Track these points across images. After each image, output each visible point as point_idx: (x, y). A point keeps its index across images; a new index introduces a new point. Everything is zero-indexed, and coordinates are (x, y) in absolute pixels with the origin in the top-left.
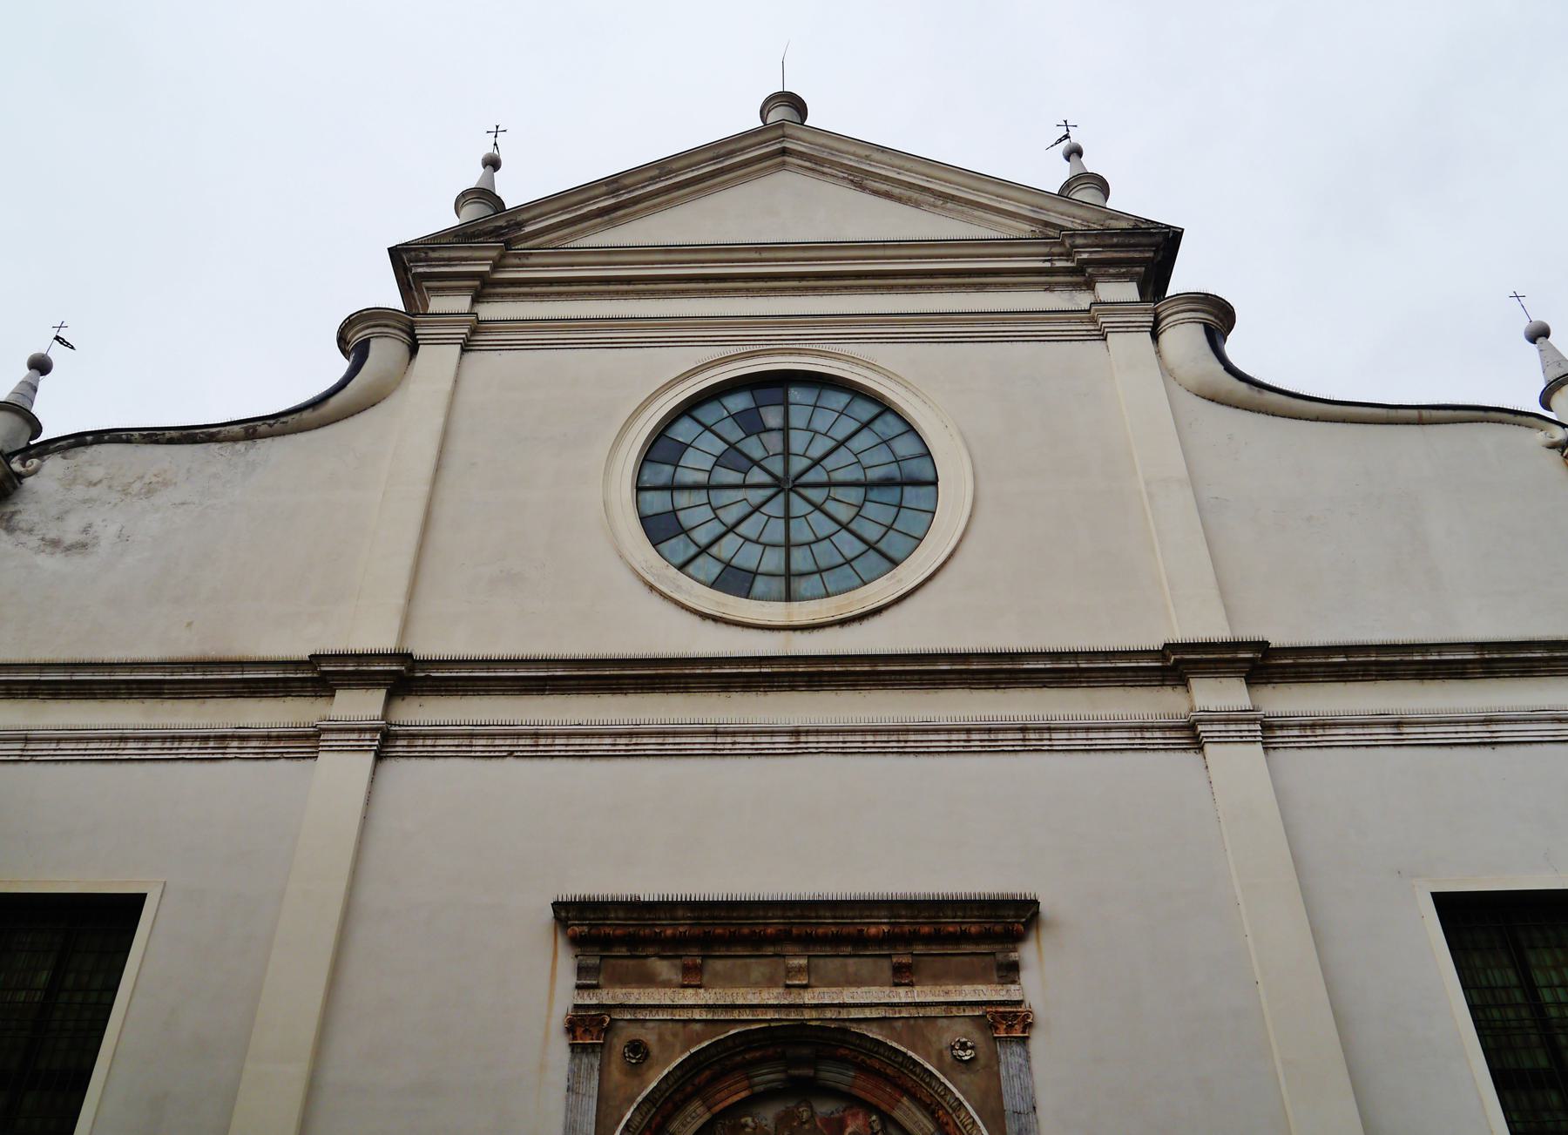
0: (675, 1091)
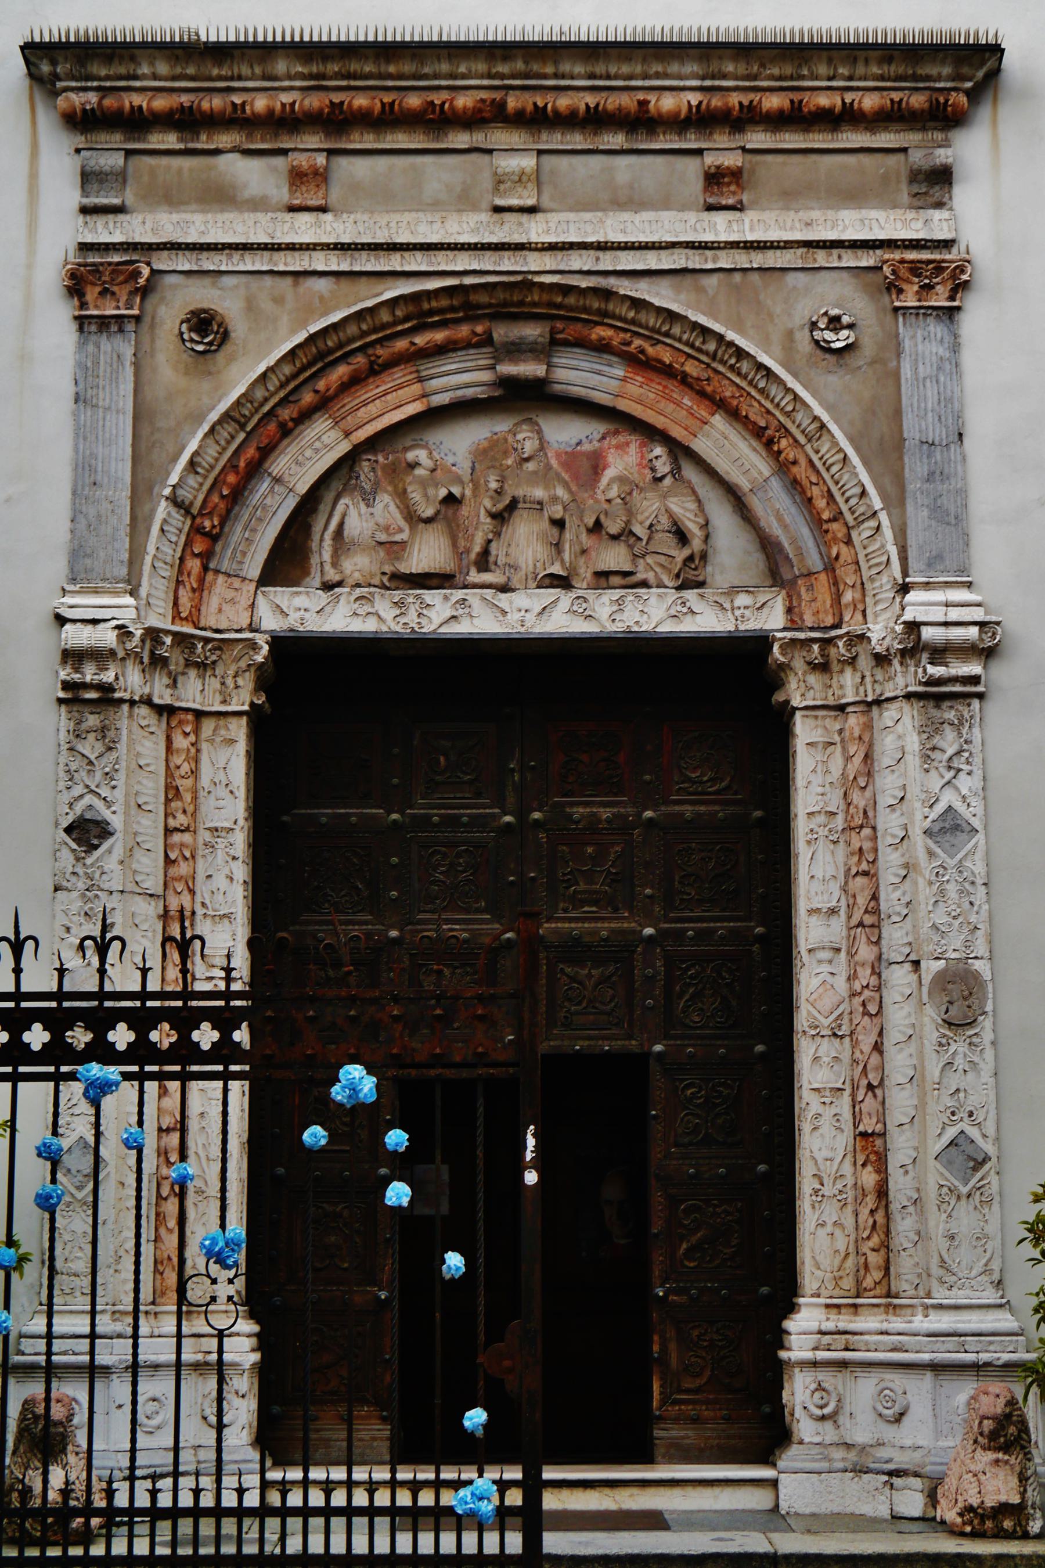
0: (284, 402)
